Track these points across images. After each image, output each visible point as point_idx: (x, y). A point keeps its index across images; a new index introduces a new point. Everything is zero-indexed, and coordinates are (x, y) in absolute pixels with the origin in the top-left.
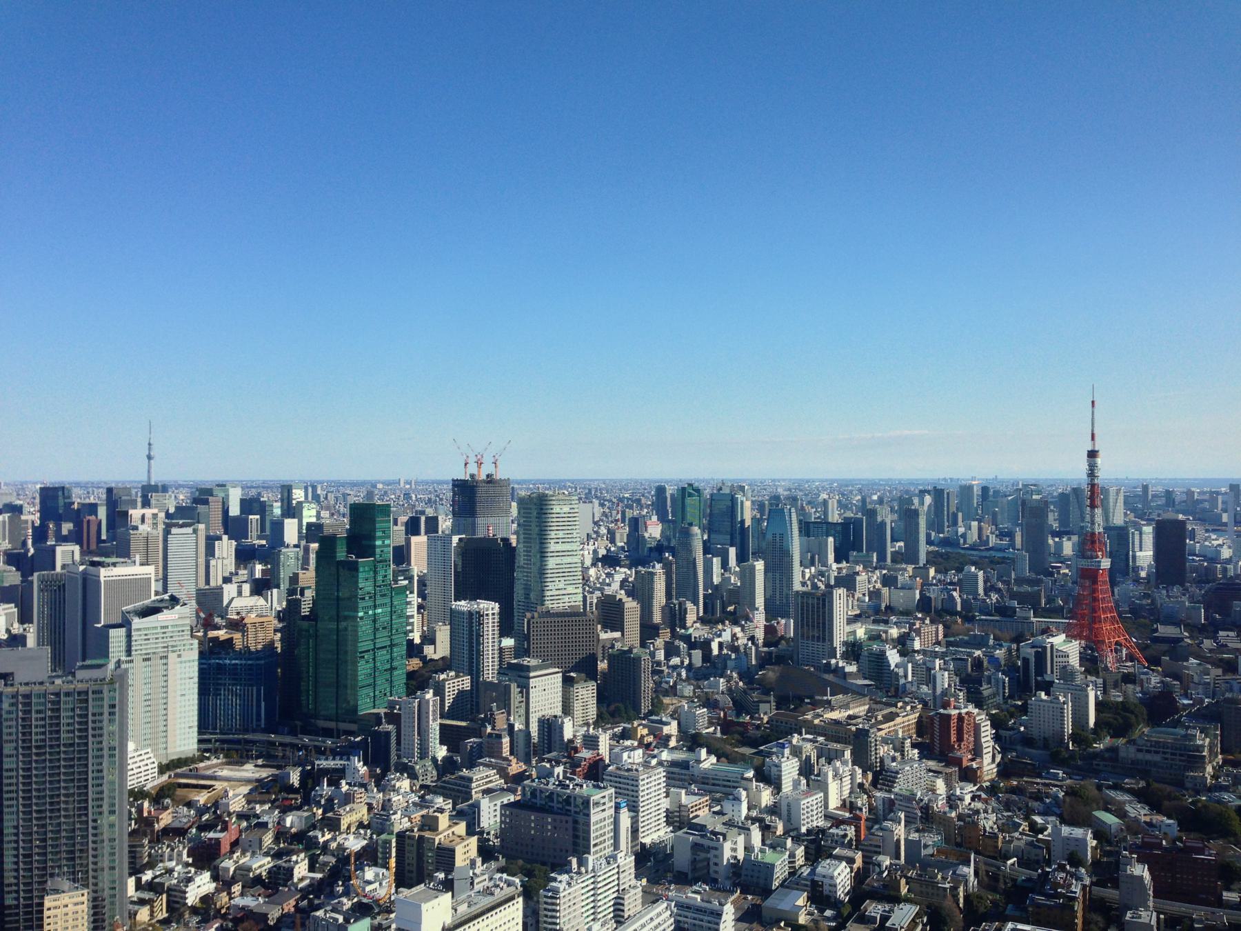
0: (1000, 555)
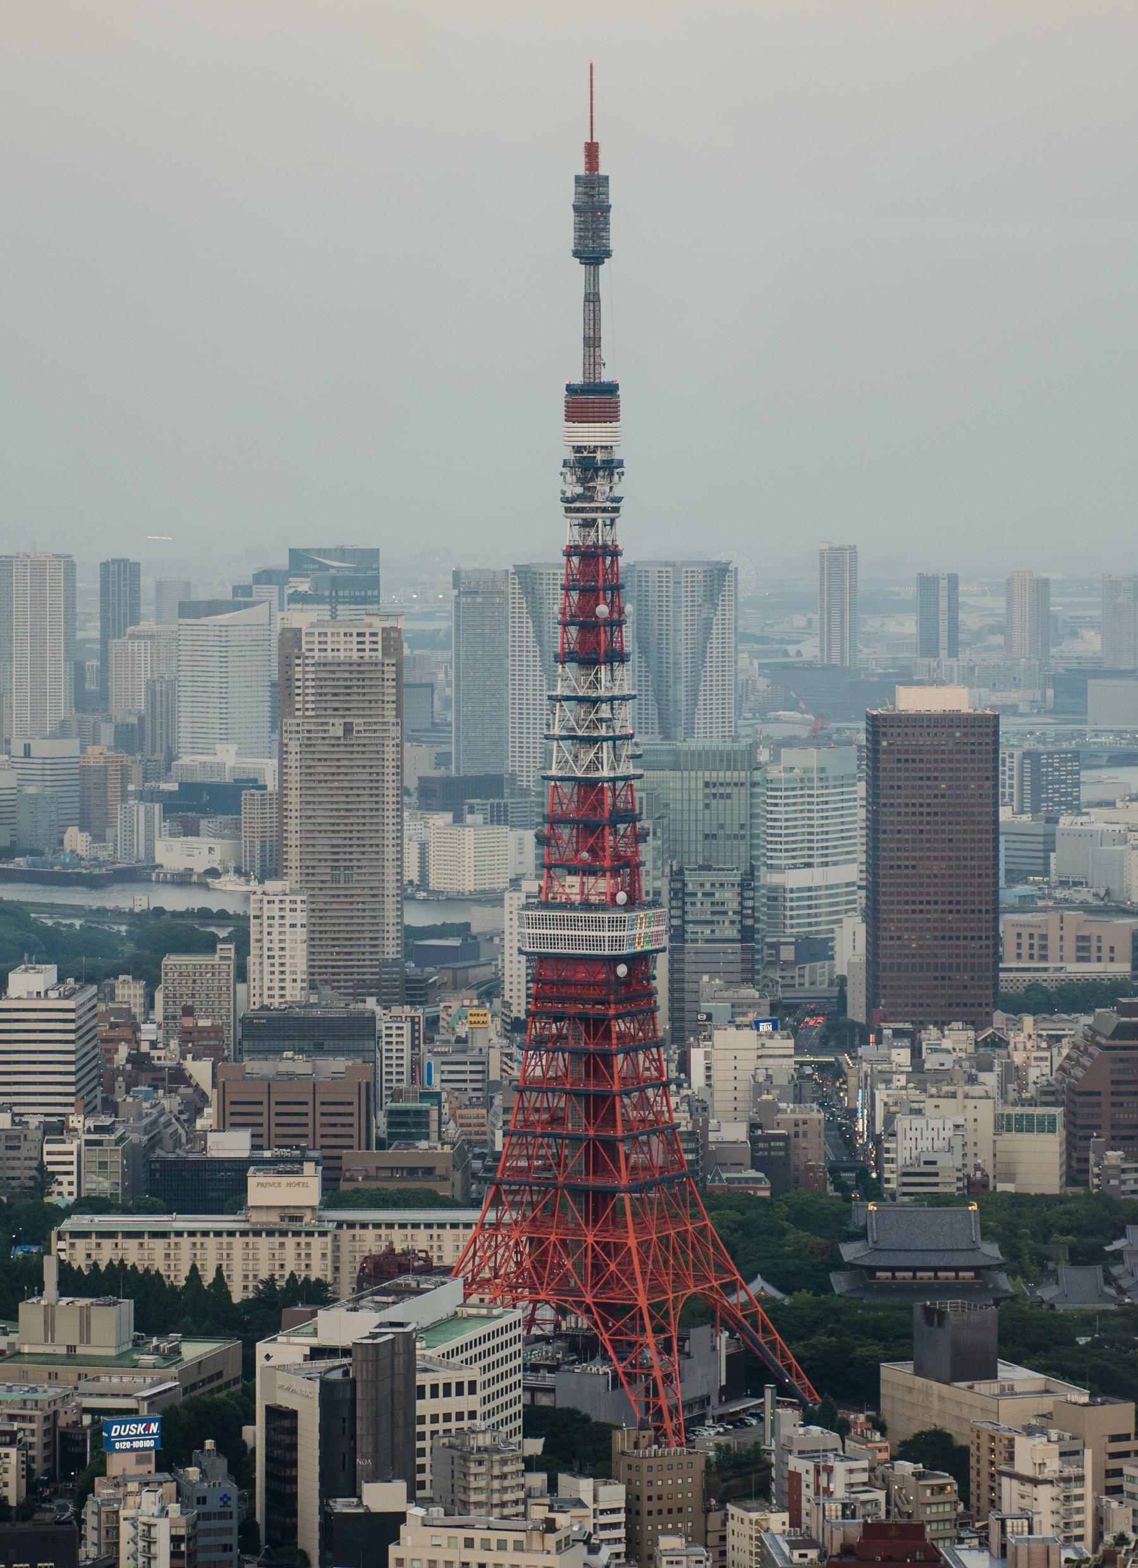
0: (175, 900)
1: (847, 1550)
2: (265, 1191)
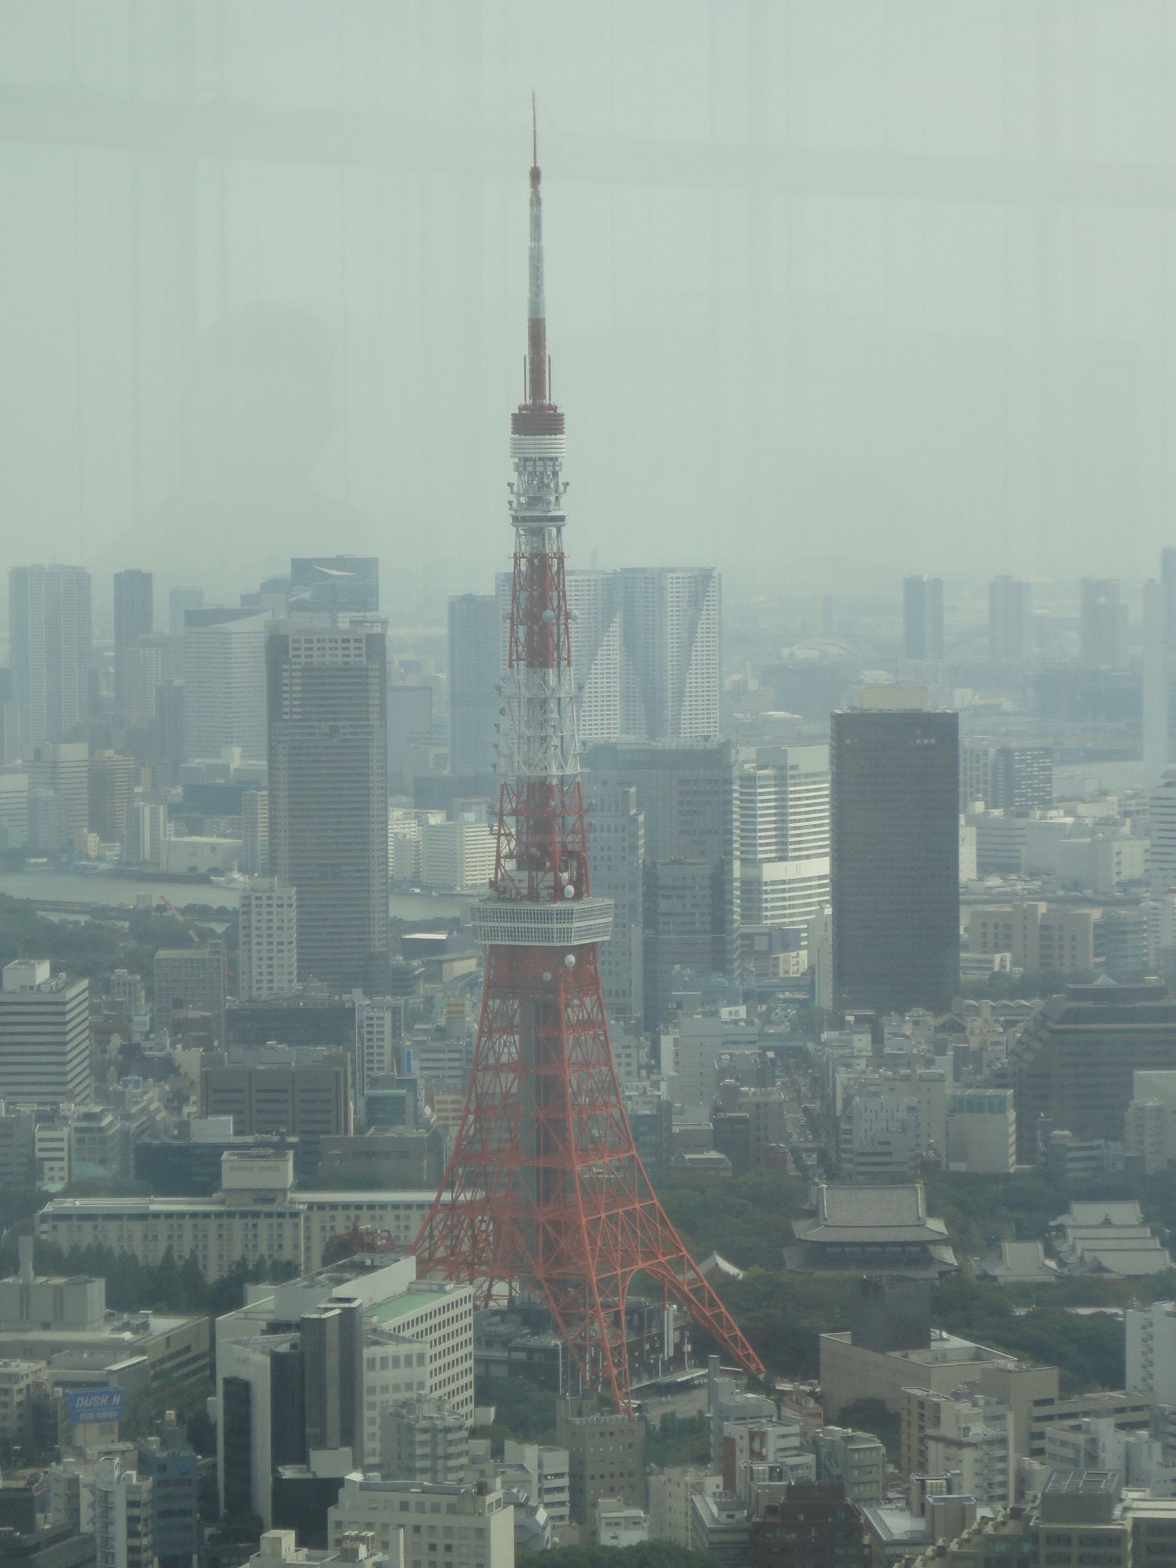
2: (236, 1174)
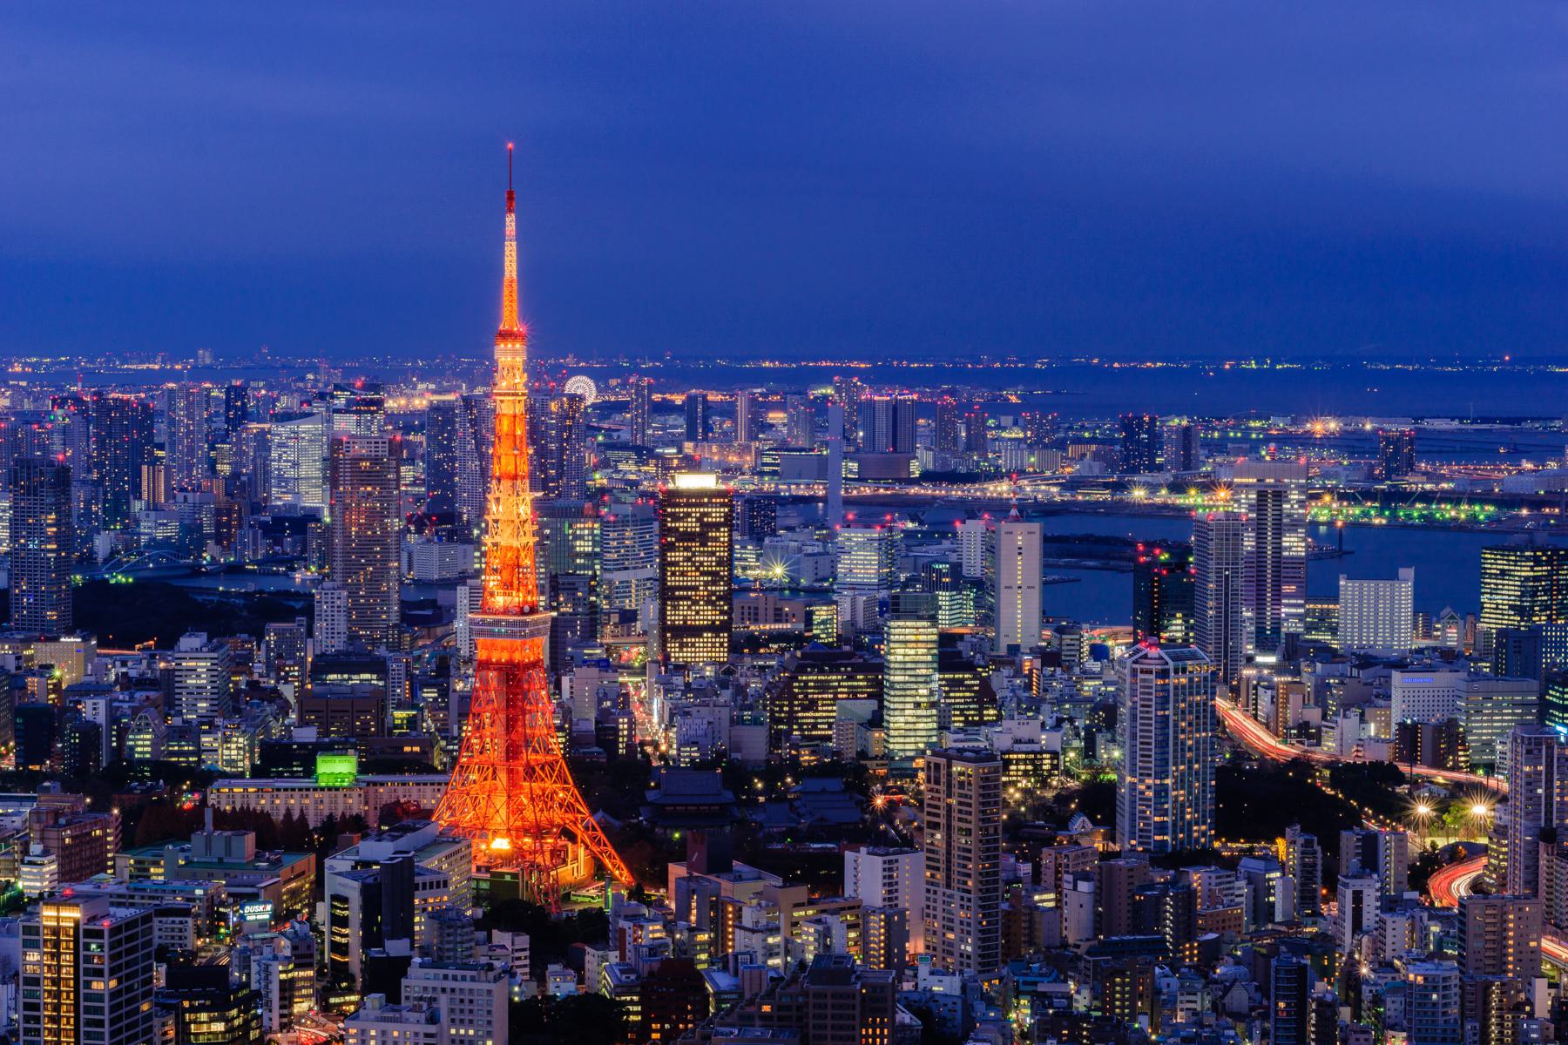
1: (651, 973)
